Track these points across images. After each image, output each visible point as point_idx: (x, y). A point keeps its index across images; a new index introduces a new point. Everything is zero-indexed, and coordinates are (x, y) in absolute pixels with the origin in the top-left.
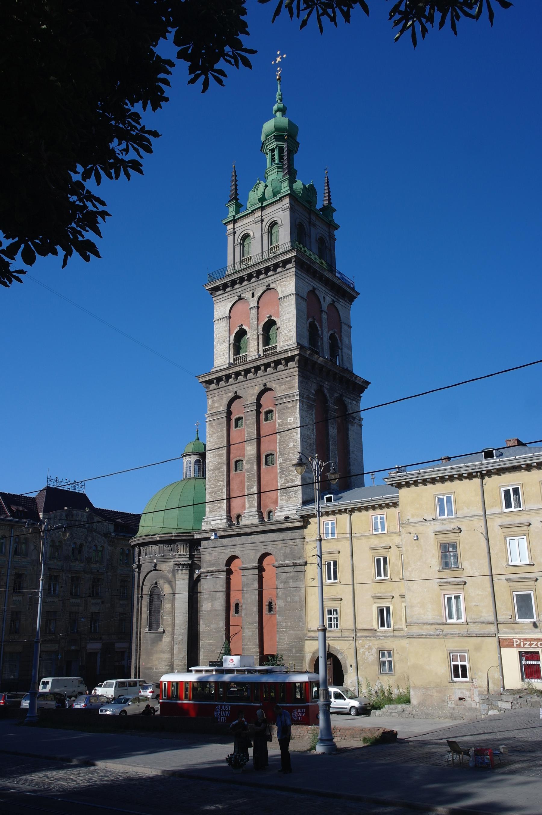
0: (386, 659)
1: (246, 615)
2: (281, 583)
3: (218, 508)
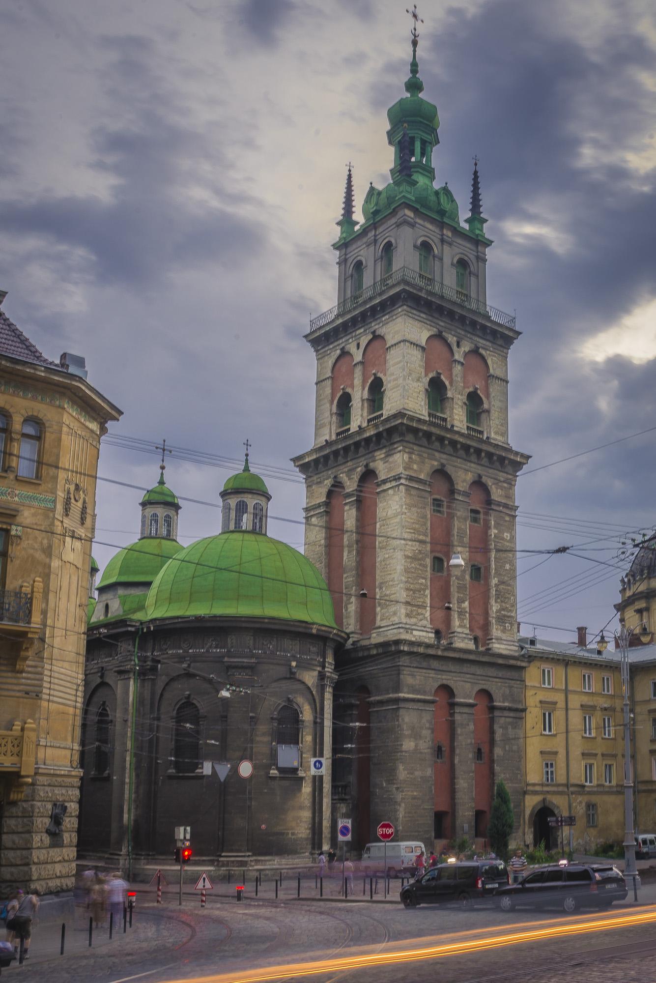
0: (591, 812)
1: (460, 762)
2: (500, 727)
3: (418, 614)
